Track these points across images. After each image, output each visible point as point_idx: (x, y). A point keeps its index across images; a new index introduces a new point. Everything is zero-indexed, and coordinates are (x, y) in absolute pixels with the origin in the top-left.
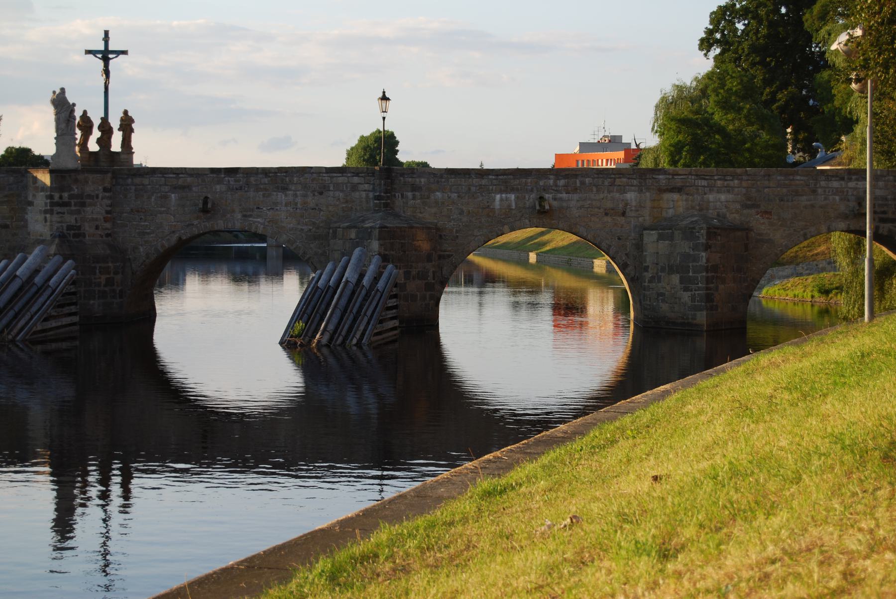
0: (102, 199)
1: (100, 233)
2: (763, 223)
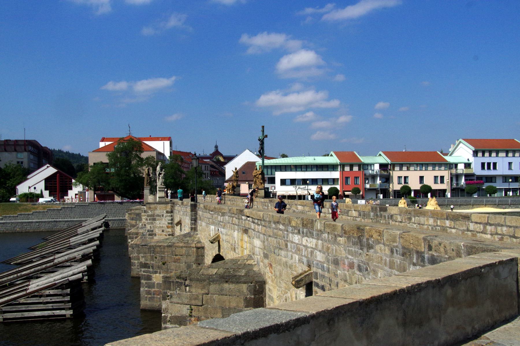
0: (166, 217)
1: (165, 234)
2: (269, 277)
